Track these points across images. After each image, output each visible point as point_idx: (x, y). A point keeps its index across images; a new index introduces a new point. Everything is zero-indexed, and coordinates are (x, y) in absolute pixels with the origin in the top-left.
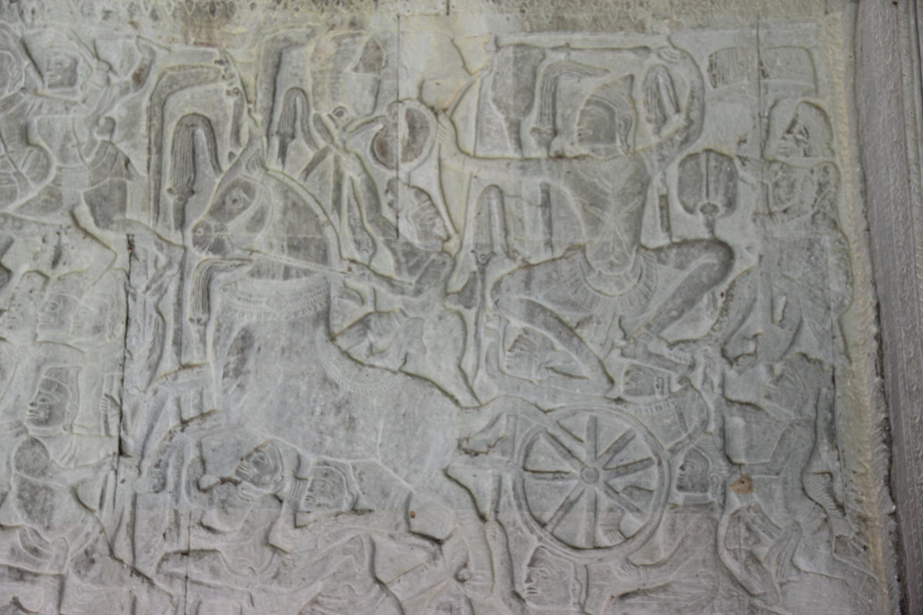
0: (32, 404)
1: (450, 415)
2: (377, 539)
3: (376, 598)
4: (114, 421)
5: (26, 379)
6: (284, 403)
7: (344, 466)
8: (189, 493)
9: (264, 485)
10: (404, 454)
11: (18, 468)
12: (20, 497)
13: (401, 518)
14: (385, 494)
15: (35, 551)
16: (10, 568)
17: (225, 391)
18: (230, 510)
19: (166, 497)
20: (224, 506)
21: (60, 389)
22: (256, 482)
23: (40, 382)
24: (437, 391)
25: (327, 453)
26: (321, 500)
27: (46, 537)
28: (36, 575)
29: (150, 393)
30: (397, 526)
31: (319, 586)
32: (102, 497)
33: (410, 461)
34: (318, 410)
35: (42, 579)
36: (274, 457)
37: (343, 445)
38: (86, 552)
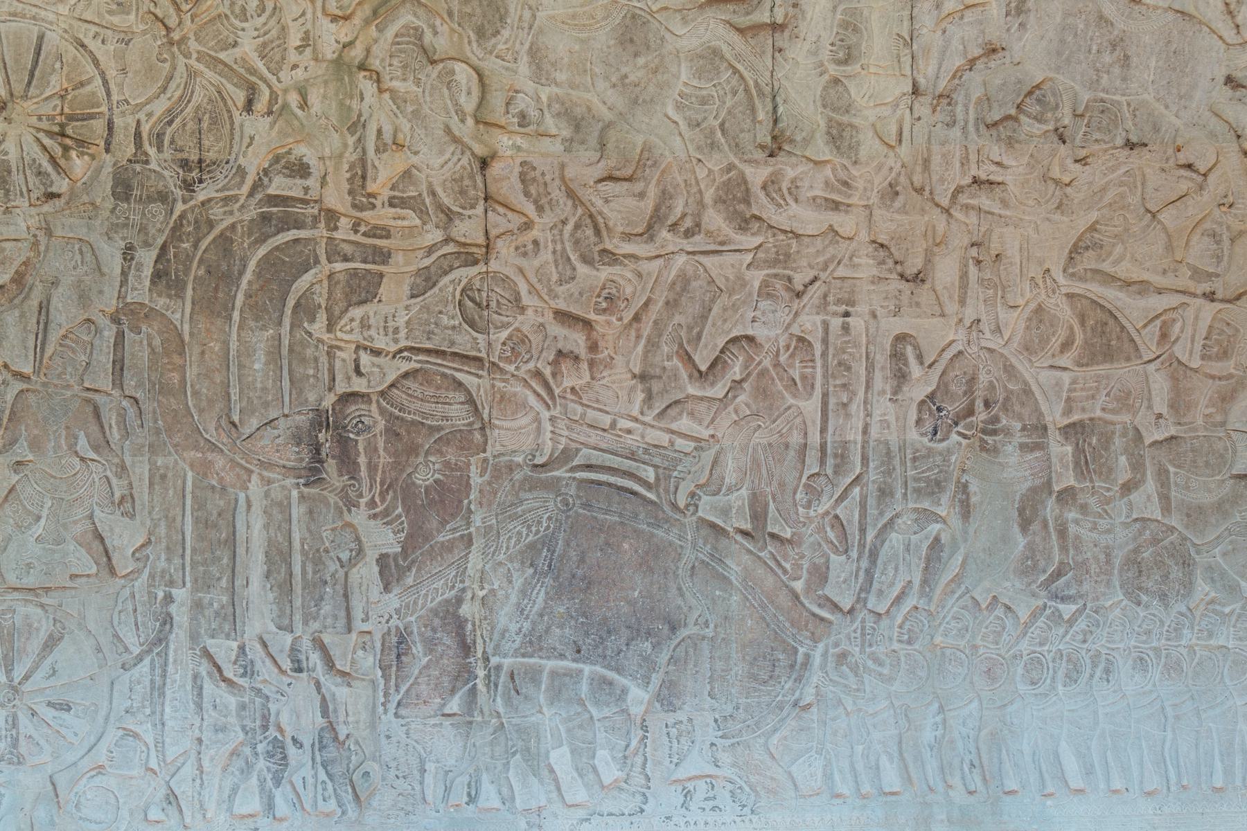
0: (832, 44)
1: (1218, 52)
2: (1148, 171)
3: (1148, 226)
4: (907, 60)
5: (825, 19)
6: (1062, 41)
7: (1118, 103)
8: (978, 130)
9: (1045, 122)
10: (1174, 91)
11: (824, 106)
12: (828, 133)
13: (1170, 151)
14: (1156, 129)
15: (846, 184)
16: (826, 199)
17: (1008, 30)
18: (1017, 146)
19: (956, 132)
20: (1010, 142)
21: (856, 30)
22: (1039, 119)
23: (836, 22)
24: (1205, 29)
25: (1103, 90)
26: (1097, 136)
27: (854, 172)
28: (849, 206)
29: (939, 33)
30: (1167, 159)
31: (1094, 216)
32: (901, 134)
33: (1181, 98)
34: (1095, 47)
35: (855, 210)
36: (1054, 94)
37: (1118, 82)
38: (890, 185)
